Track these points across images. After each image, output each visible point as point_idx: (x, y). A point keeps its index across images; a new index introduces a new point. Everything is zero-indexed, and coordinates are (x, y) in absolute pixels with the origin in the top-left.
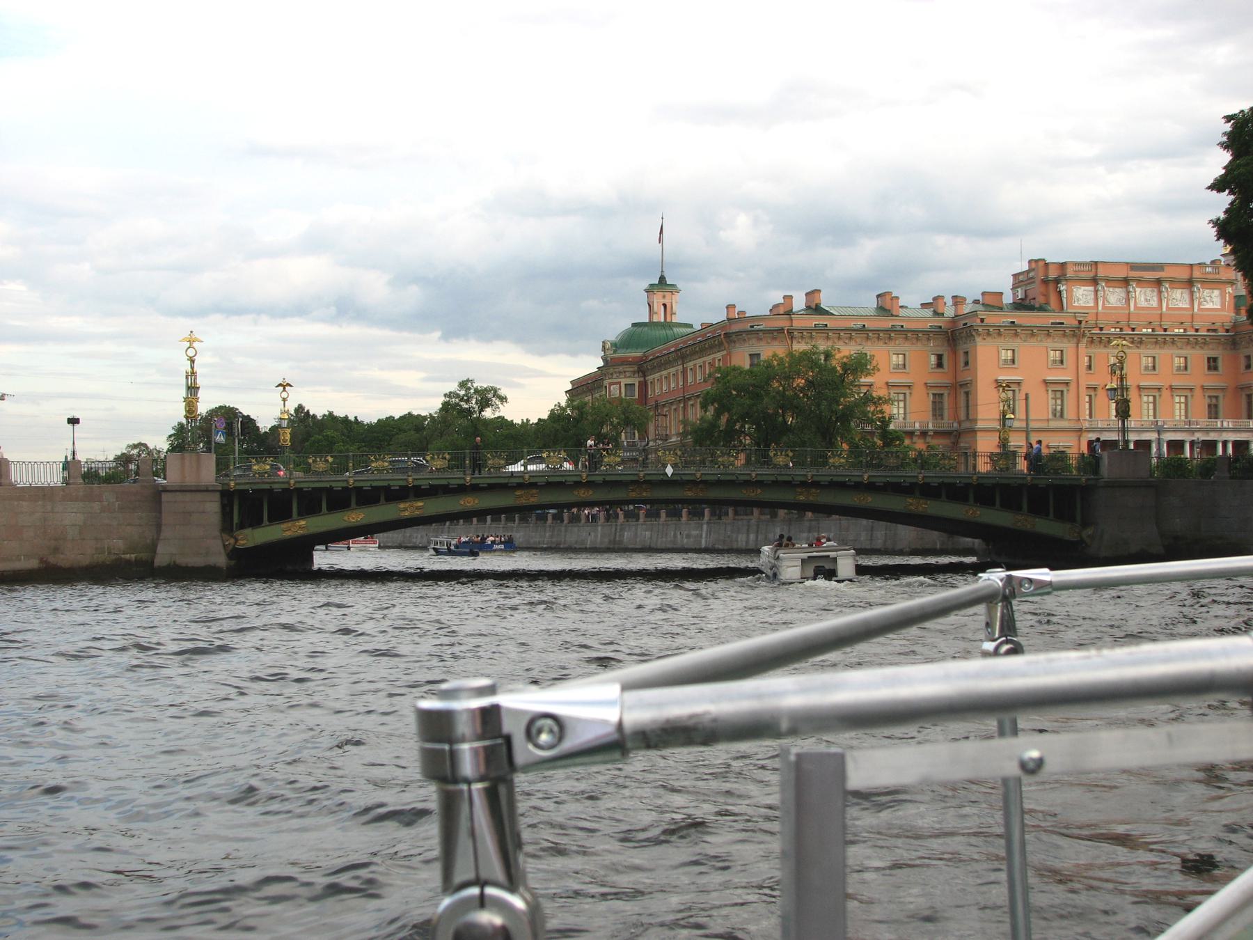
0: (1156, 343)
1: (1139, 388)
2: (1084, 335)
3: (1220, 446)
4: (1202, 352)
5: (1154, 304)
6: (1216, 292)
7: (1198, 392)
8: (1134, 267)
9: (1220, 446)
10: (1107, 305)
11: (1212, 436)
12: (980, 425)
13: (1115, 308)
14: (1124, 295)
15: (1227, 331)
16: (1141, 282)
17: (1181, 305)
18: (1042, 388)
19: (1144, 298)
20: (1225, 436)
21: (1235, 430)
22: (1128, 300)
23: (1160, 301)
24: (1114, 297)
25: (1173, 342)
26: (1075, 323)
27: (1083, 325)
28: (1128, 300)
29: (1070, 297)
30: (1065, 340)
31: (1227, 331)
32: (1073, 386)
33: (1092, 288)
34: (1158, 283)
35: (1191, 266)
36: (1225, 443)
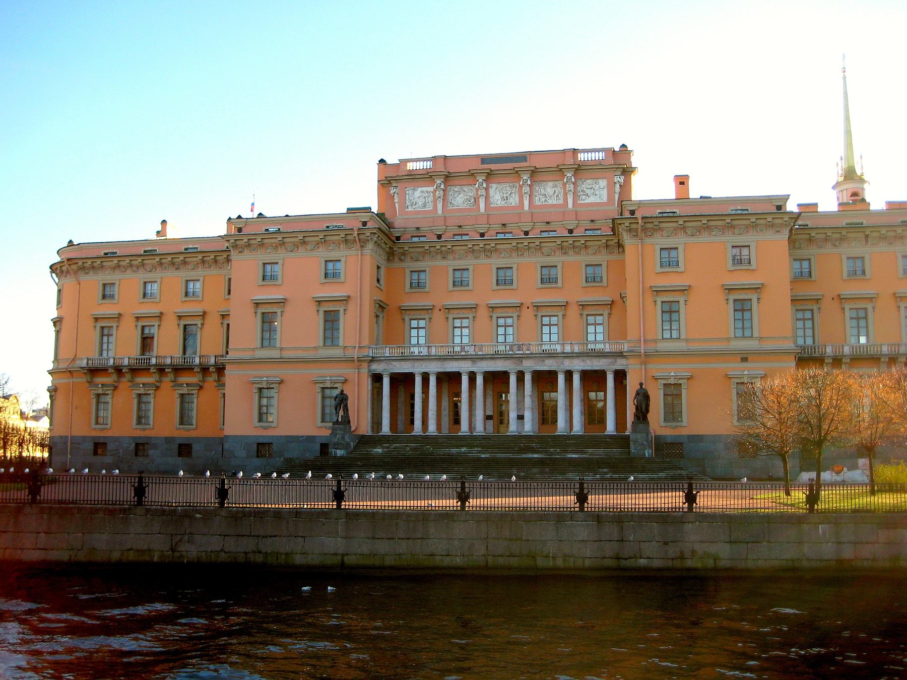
1: (493, 308)
4: (578, 258)
6: (603, 183)
8: (485, 159)
13: (460, 210)
17: (550, 202)
18: (313, 307)
19: (501, 196)
20: (568, 364)
21: (580, 355)
22: (476, 200)
24: (460, 198)
25: (539, 248)
32: (353, 307)
33: (431, 189)
35: (564, 151)
36: (569, 374)
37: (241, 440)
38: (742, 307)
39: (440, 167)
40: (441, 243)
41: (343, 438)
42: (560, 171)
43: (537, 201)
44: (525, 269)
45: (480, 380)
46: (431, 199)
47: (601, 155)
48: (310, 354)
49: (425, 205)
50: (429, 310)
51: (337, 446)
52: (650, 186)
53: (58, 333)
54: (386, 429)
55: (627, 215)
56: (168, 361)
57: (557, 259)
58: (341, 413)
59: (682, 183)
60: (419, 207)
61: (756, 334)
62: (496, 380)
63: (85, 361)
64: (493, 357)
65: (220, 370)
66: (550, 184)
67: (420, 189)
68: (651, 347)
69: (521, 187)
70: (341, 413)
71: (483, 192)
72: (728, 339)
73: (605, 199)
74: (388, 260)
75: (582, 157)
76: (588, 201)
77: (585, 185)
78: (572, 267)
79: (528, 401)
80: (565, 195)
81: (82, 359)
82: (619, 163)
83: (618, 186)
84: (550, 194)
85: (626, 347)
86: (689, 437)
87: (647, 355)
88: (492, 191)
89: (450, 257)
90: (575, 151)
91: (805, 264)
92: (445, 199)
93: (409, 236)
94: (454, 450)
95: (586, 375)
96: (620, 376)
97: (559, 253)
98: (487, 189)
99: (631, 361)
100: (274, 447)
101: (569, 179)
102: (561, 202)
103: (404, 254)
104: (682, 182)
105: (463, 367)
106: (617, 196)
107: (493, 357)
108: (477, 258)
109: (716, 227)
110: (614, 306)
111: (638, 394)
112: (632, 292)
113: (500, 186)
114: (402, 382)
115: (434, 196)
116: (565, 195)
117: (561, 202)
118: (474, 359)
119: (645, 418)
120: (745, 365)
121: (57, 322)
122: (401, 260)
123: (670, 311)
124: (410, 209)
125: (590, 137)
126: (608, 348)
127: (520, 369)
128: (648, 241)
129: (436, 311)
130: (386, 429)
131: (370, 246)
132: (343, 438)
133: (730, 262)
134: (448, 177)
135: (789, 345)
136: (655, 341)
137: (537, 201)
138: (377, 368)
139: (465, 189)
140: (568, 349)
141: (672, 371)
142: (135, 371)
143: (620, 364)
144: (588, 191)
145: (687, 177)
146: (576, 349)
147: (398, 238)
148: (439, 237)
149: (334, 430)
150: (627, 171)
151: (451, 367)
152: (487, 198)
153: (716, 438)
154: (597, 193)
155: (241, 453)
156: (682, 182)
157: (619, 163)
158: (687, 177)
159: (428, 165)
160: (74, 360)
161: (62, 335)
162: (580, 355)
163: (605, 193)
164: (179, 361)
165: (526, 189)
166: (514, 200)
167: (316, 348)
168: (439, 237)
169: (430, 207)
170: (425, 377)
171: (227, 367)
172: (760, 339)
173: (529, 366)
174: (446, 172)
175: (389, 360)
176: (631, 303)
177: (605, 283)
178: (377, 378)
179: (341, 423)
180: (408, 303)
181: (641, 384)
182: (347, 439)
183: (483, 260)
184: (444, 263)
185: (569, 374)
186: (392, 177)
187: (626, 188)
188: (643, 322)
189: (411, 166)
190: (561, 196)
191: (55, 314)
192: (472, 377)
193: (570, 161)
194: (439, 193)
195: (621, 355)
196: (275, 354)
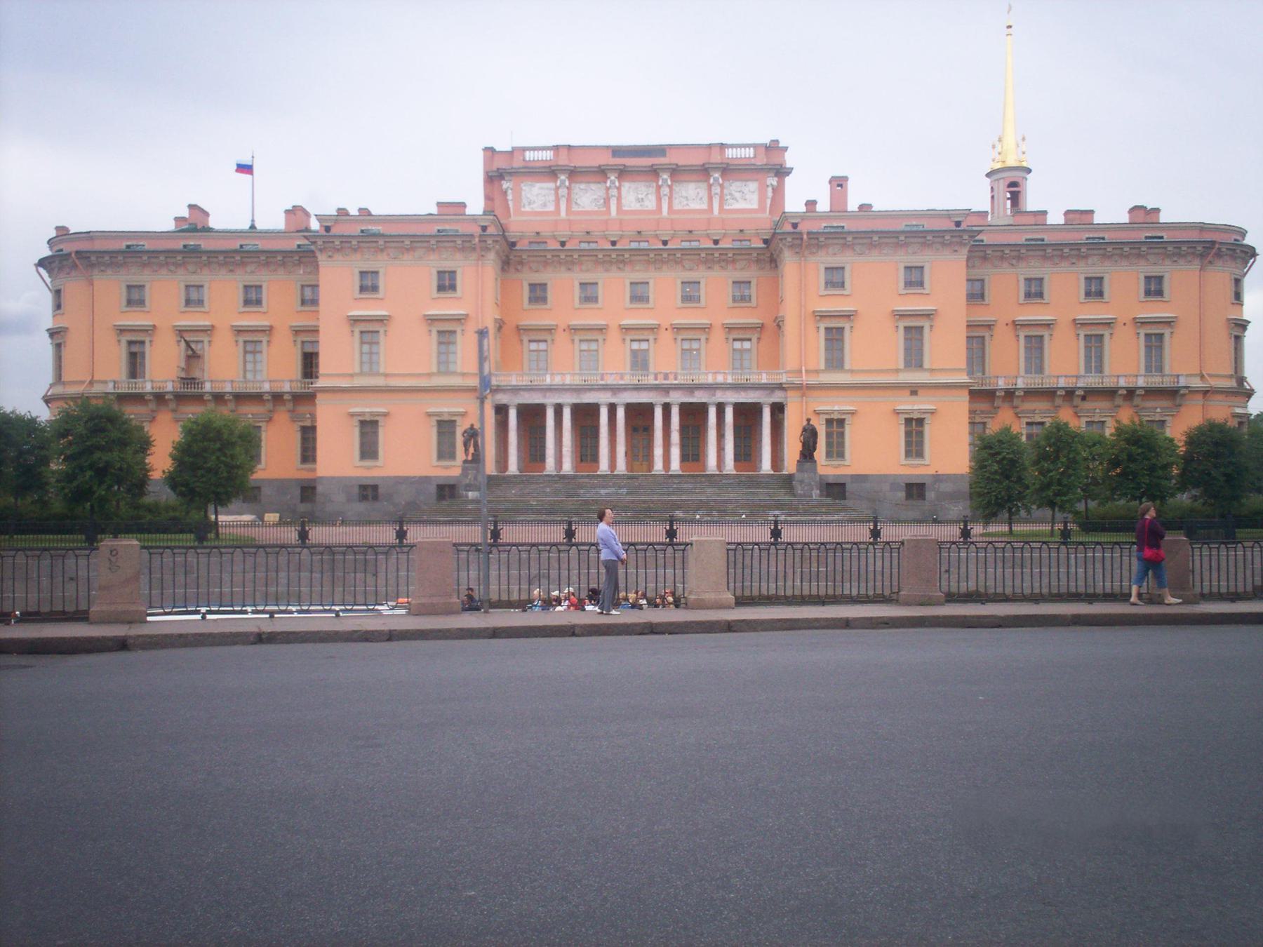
0: (648, 262)
2: (488, 249)
3: (712, 412)
5: (650, 204)
6: (753, 186)
7: (718, 336)
8: (617, 151)
9: (712, 412)
10: (575, 208)
11: (699, 397)
12: (320, 383)
14: (602, 193)
15: (765, 241)
16: (623, 173)
17: (693, 206)
19: (636, 197)
20: (720, 397)
21: (736, 387)
22: (607, 201)
23: (659, 200)
24: (588, 197)
25: (679, 262)
26: (478, 231)
27: (491, 230)
28: (607, 201)
30: (458, 256)
31: (765, 241)
33: (552, 185)
34: (654, 172)
35: (710, 146)
36: (721, 408)
37: (342, 483)
38: (914, 336)
39: (563, 160)
40: (565, 253)
41: (475, 479)
42: (704, 172)
43: (676, 206)
44: (665, 285)
45: (621, 413)
46: (552, 198)
47: (750, 153)
48: (424, 383)
49: (545, 205)
50: (549, 330)
51: (469, 487)
52: (803, 191)
53: (58, 347)
54: (513, 467)
55: (788, 228)
56: (228, 389)
57: (699, 274)
58: (471, 450)
59: (841, 186)
60: (536, 207)
61: (926, 365)
62: (639, 417)
63: (111, 385)
64: (638, 388)
65: (305, 399)
66: (692, 186)
67: (538, 185)
68: (813, 380)
69: (659, 188)
70: (471, 450)
71: (614, 192)
72: (897, 371)
73: (755, 206)
74: (503, 270)
75: (730, 153)
77: (734, 187)
78: (716, 285)
79: (675, 437)
80: (710, 198)
81: (105, 382)
82: (770, 165)
83: (770, 189)
84: (691, 197)
85: (784, 379)
86: (852, 476)
87: (810, 387)
89: (576, 268)
90: (723, 146)
91: (978, 285)
92: (569, 200)
93: (526, 242)
94: (603, 492)
95: (740, 409)
96: (778, 409)
97: (702, 267)
98: (619, 189)
99: (790, 393)
100: (381, 491)
101: (716, 180)
102: (705, 206)
103: (521, 263)
104: (839, 183)
105: (603, 398)
106: (769, 201)
107: (638, 388)
108: (607, 270)
109: (887, 244)
110: (768, 331)
111: (804, 430)
112: (790, 312)
113: (633, 185)
114: (532, 416)
115: (557, 194)
116: (710, 198)
117: (705, 206)
118: (615, 389)
119: (811, 456)
120: (914, 398)
121: (53, 333)
122: (517, 270)
123: (835, 337)
124: (527, 209)
125: (739, 130)
126: (764, 379)
127: (667, 400)
128: (813, 259)
129: (560, 330)
130: (513, 467)
131: (492, 256)
132: (475, 479)
133: (902, 284)
134: (574, 173)
135: (963, 378)
136: (817, 372)
137: (676, 206)
138: (503, 399)
139: (593, 186)
140: (720, 379)
141: (836, 404)
142: (180, 398)
143: (777, 397)
144: (737, 195)
145: (845, 179)
146: (730, 380)
147: (513, 244)
148: (563, 244)
149: (465, 470)
150: (782, 172)
151: (588, 398)
152: (619, 198)
153: (882, 478)
154: (745, 198)
155: (340, 498)
156: (839, 183)
157: (770, 165)
158: (845, 179)
159: (548, 155)
160: (91, 383)
161: (65, 353)
162: (736, 387)
163: (755, 197)
164: (240, 388)
165: (665, 190)
166: (650, 204)
167: (430, 375)
168: (563, 244)
169: (551, 208)
170: (559, 409)
171: (319, 396)
172: (932, 371)
173: (676, 398)
174: (569, 167)
175: (516, 390)
176: (790, 327)
177: (754, 303)
178: (501, 410)
179: (471, 462)
180: (527, 321)
181: (809, 420)
182: (480, 478)
183: (614, 274)
185: (721, 408)
186: (502, 171)
187: (779, 192)
188: (802, 352)
189: (529, 156)
190: (706, 199)
191: (50, 324)
192: (612, 408)
193: (716, 158)
194: (563, 192)
195: (780, 387)
196: (380, 382)
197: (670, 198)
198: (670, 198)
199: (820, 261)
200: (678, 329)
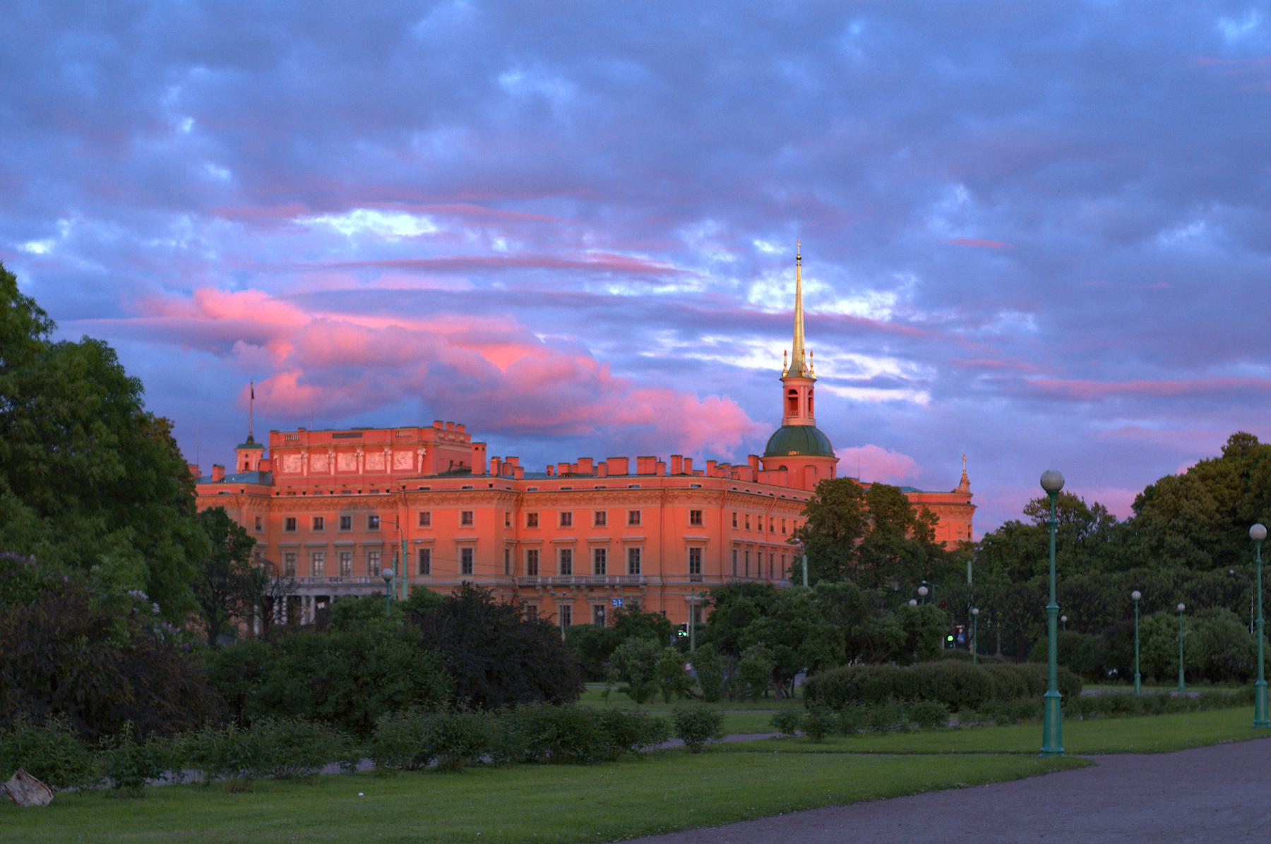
6: (410, 454)
13: (319, 473)
16: (337, 449)
29: (282, 463)
34: (352, 449)
43: (368, 467)
60: (291, 470)
76: (401, 468)
83: (420, 458)
88: (339, 459)
98: (336, 458)
107: (319, 586)
128: (412, 508)
140: (363, 581)
152: (336, 464)
165: (361, 459)
166: (353, 467)
169: (299, 470)
184: (306, 513)
197: (364, 464)
198: (364, 464)
199: (417, 510)
200: (366, 546)
